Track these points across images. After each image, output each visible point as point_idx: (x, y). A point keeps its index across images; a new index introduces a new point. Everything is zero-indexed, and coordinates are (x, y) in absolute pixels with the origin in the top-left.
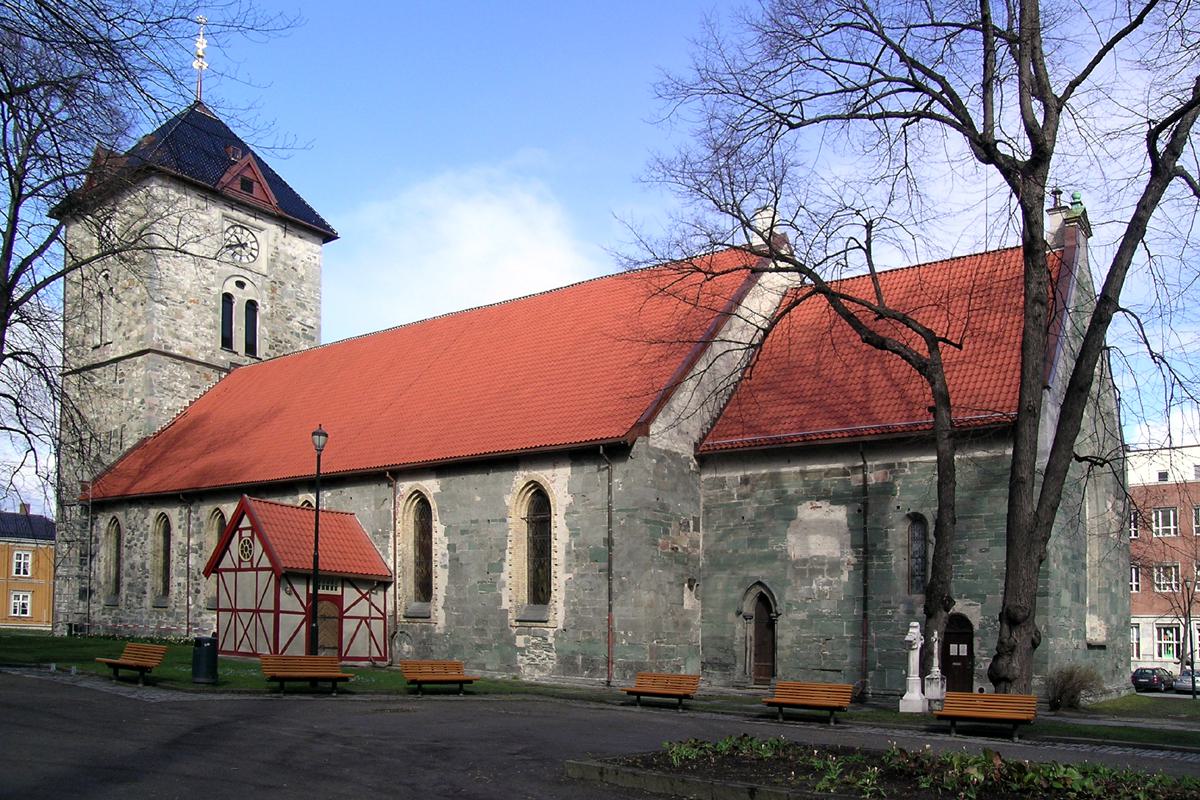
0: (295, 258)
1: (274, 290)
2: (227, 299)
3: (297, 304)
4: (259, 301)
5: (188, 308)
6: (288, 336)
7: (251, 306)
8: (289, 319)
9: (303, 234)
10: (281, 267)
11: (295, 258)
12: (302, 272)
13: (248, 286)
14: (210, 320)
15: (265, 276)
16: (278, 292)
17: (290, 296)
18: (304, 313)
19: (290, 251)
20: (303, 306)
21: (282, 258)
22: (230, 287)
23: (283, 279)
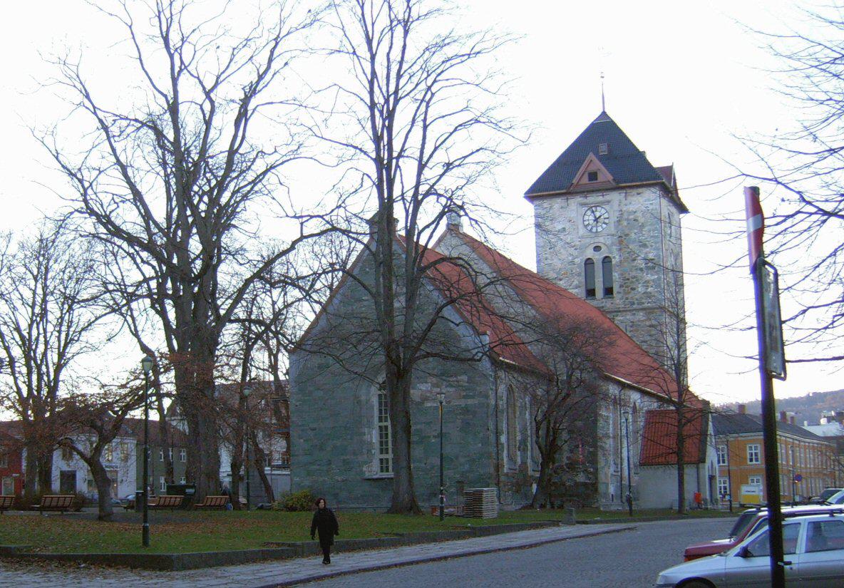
0: (635, 212)
1: (621, 242)
2: (589, 263)
3: (640, 246)
4: (610, 255)
5: (561, 280)
6: (634, 273)
7: (607, 260)
8: (634, 260)
9: (640, 190)
10: (625, 223)
11: (635, 212)
12: (641, 220)
13: (604, 248)
14: (576, 282)
15: (613, 235)
16: (625, 241)
17: (634, 242)
18: (645, 250)
19: (631, 208)
20: (645, 246)
21: (625, 216)
22: (590, 253)
23: (627, 232)
